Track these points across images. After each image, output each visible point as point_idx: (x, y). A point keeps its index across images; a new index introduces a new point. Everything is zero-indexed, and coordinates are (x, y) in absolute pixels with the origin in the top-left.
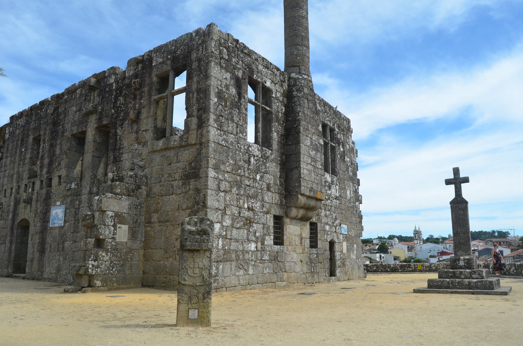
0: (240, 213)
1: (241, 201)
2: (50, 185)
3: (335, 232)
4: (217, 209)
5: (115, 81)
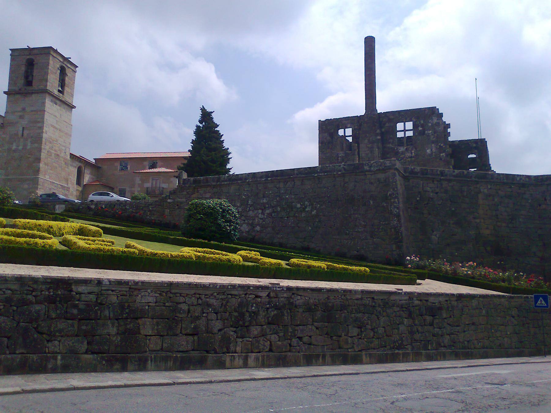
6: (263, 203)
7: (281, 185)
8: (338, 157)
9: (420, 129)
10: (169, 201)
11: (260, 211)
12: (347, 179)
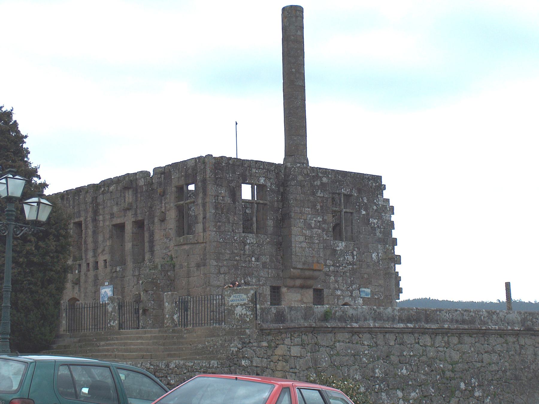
2: (96, 267)
3: (351, 296)
4: (218, 287)
5: (144, 184)
6: (402, 376)
9: (364, 212)
12: (522, 341)
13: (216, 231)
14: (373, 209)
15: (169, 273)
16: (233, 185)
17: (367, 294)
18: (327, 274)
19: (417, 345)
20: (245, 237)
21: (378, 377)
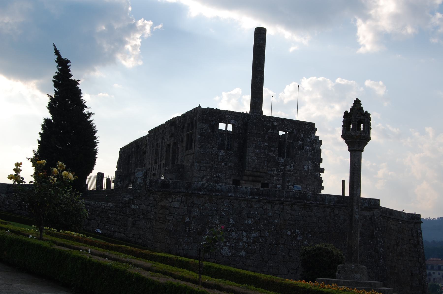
0: (211, 178)
1: (212, 174)
4: (199, 177)
7: (269, 207)
8: (218, 156)
9: (301, 143)
10: (133, 206)
11: (245, 234)
13: (200, 148)
14: (307, 141)
15: (180, 170)
16: (213, 123)
17: (298, 188)
18: (272, 175)
19: (261, 209)
20: (218, 152)
21: (231, 224)
